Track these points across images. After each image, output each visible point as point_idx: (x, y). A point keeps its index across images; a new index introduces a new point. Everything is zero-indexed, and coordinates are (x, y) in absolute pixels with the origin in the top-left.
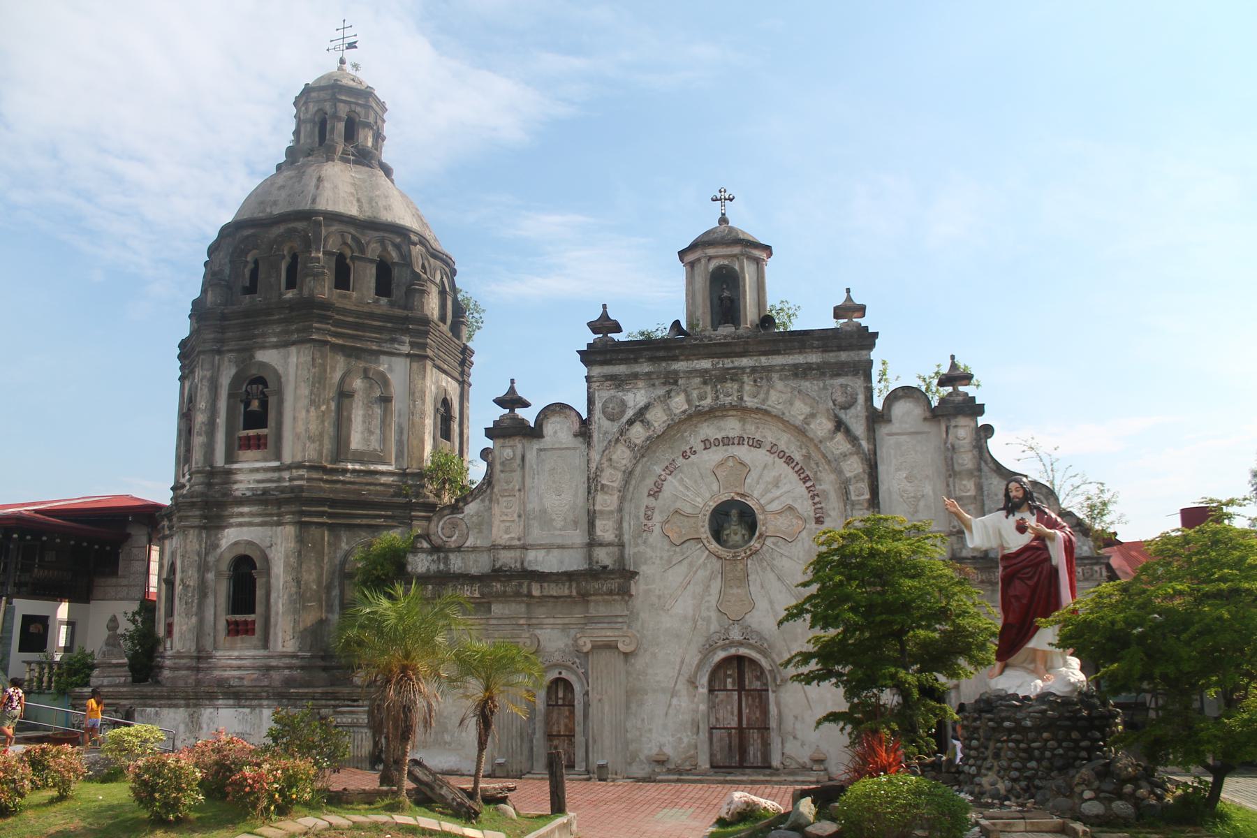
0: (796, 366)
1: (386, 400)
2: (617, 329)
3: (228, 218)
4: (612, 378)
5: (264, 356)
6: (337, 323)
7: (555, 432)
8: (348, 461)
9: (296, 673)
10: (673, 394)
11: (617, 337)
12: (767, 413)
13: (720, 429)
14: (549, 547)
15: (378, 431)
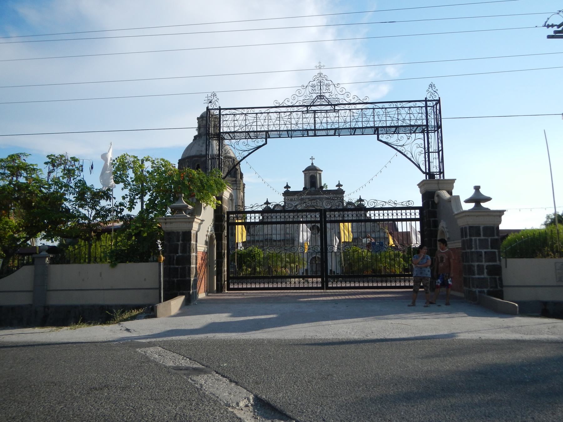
2: (290, 187)
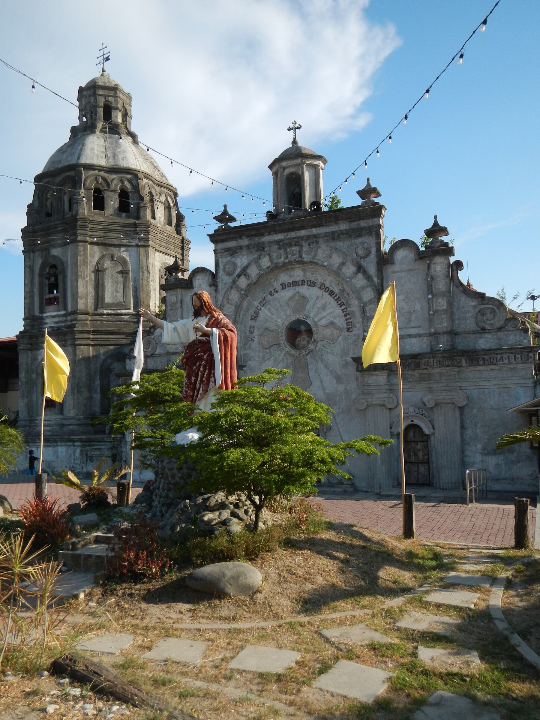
0: (333, 233)
1: (124, 273)
3: (40, 172)
4: (227, 250)
5: (56, 252)
6: (92, 230)
7: (200, 285)
8: (104, 308)
9: (76, 428)
10: (262, 257)
11: (232, 225)
12: (316, 264)
13: (291, 276)
15: (122, 291)
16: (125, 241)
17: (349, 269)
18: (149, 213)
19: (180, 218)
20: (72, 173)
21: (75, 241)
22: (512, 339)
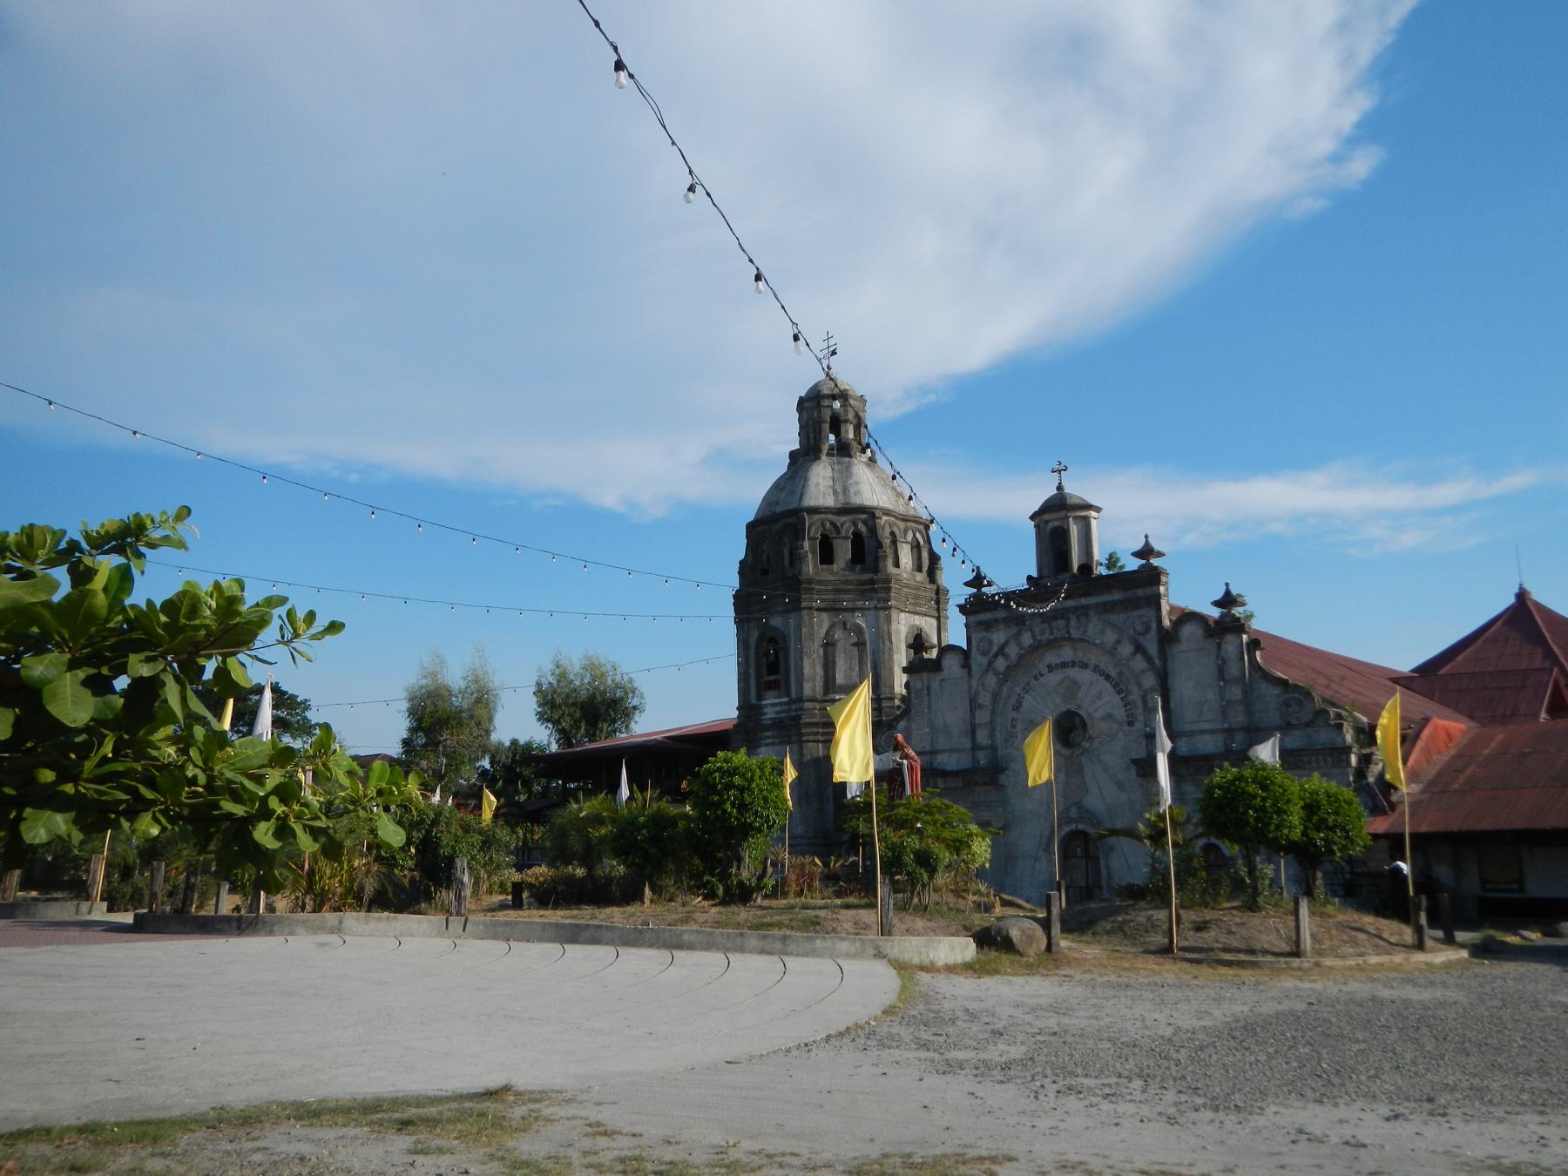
0: (1105, 603)
1: (860, 645)
2: (990, 584)
4: (981, 623)
5: (776, 621)
6: (819, 592)
8: (835, 692)
14: (951, 751)
16: (860, 603)
17: (1126, 649)
18: (890, 562)
19: (934, 558)
20: (793, 520)
21: (799, 609)
22: (1323, 736)
